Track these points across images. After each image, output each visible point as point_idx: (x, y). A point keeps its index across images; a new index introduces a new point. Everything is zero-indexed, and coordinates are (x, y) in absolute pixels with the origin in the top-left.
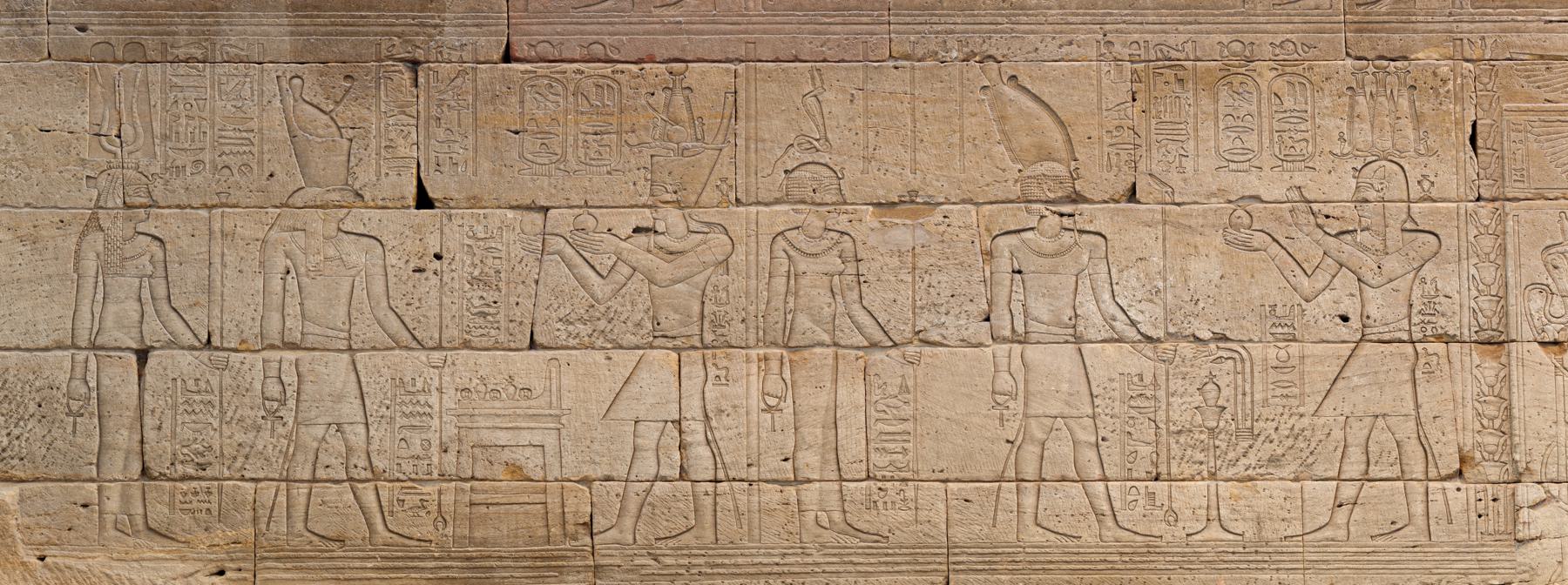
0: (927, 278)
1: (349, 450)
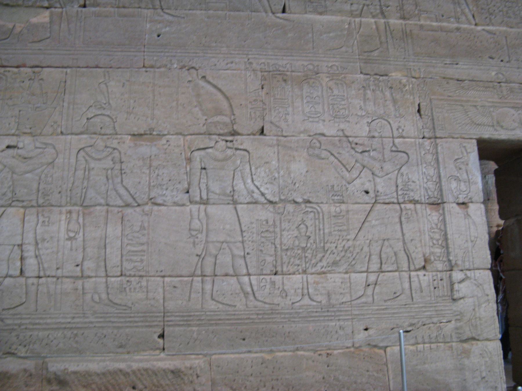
0: (157, 172)
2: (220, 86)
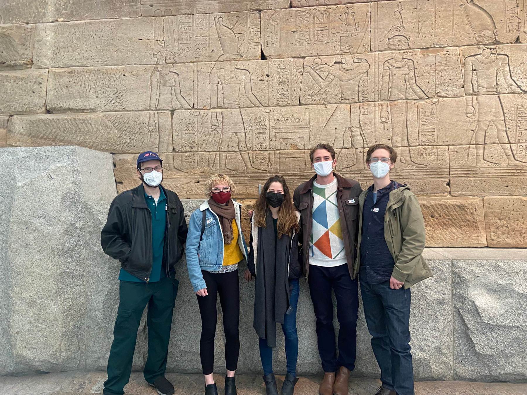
0: (440, 74)
1: (239, 141)
2: (484, 8)
